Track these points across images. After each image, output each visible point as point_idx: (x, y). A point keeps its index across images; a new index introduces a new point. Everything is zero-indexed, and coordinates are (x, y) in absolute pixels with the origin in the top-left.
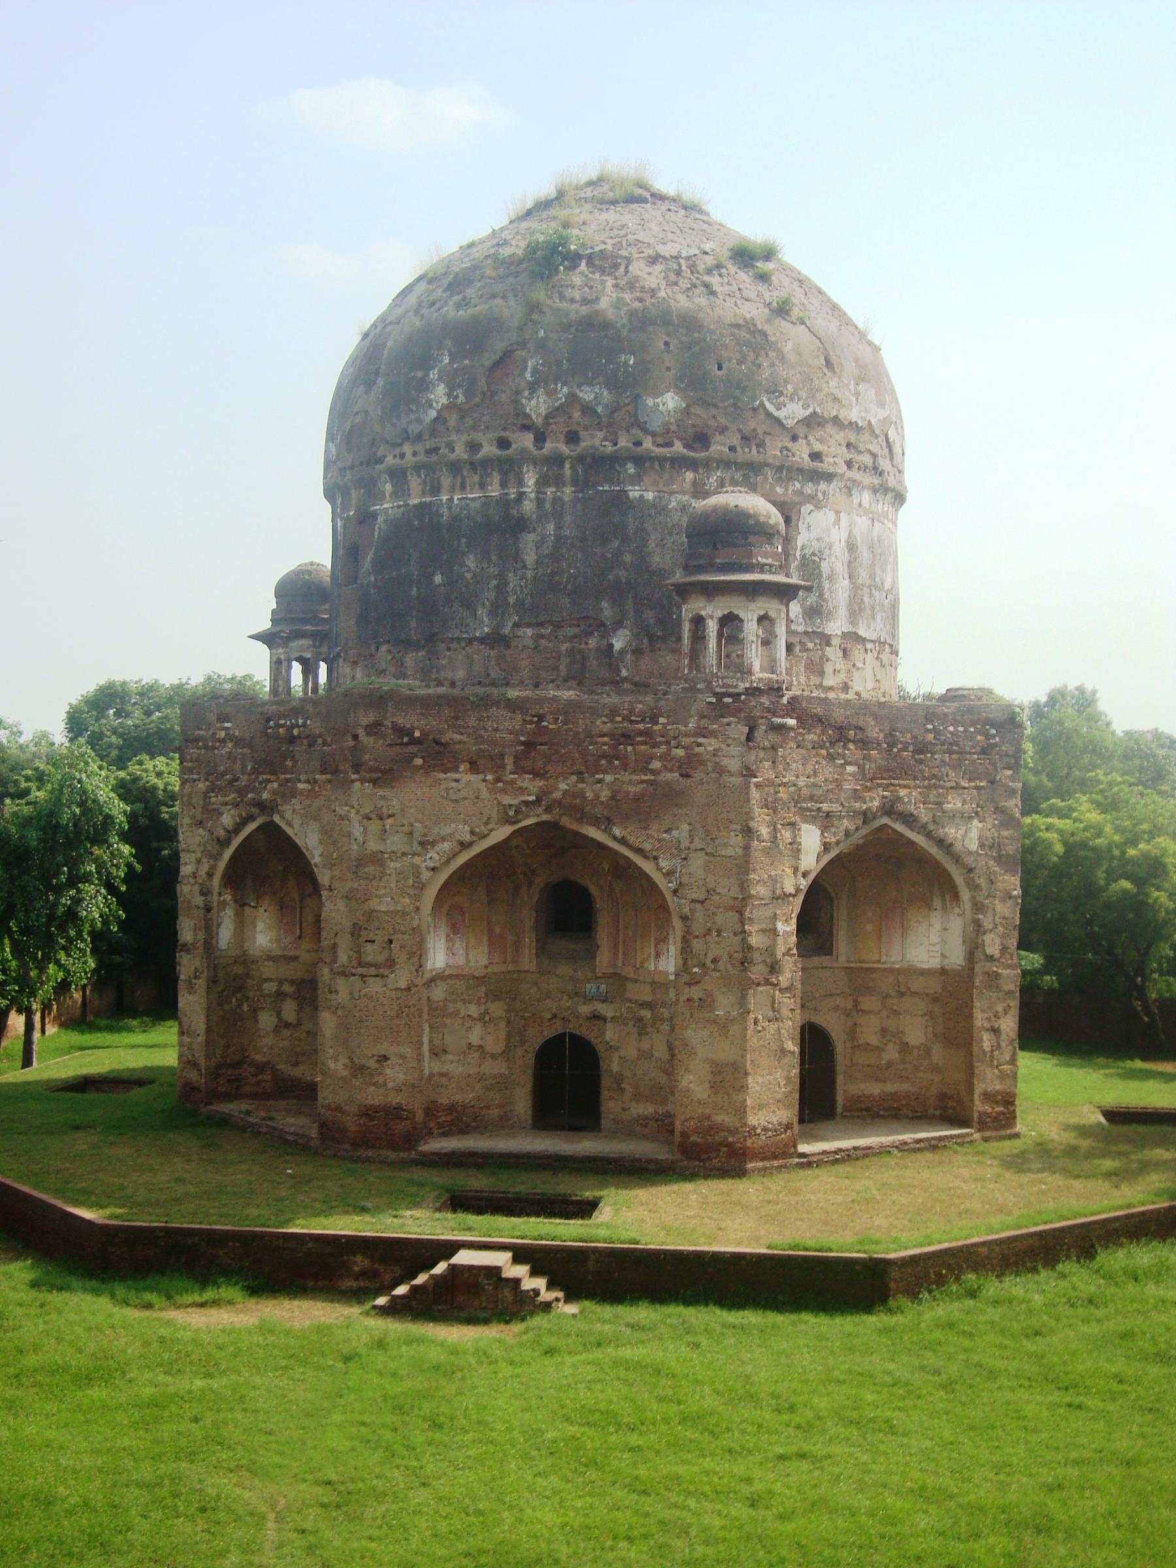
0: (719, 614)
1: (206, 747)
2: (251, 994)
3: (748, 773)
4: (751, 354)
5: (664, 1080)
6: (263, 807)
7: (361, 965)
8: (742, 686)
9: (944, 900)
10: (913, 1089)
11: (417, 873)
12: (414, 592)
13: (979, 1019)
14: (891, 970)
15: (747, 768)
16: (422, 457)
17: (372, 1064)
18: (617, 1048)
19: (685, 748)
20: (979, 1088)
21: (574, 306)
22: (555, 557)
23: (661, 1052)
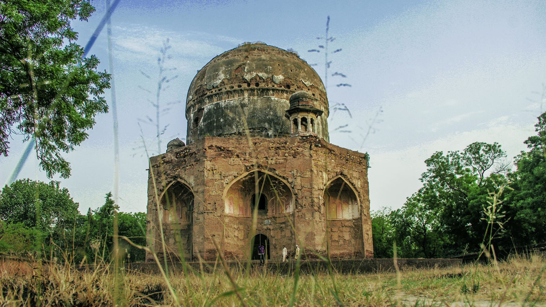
0: (301, 117)
1: (157, 167)
2: (167, 234)
3: (311, 156)
4: (298, 70)
5: (290, 242)
6: (175, 178)
7: (206, 210)
8: (308, 135)
9: (352, 201)
10: (348, 252)
11: (222, 183)
12: (215, 124)
13: (364, 230)
14: (340, 220)
15: (311, 155)
16: (217, 92)
17: (210, 237)
18: (274, 237)
19: (294, 150)
20: (365, 249)
21: (256, 57)
22: (253, 112)
23: (288, 234)
